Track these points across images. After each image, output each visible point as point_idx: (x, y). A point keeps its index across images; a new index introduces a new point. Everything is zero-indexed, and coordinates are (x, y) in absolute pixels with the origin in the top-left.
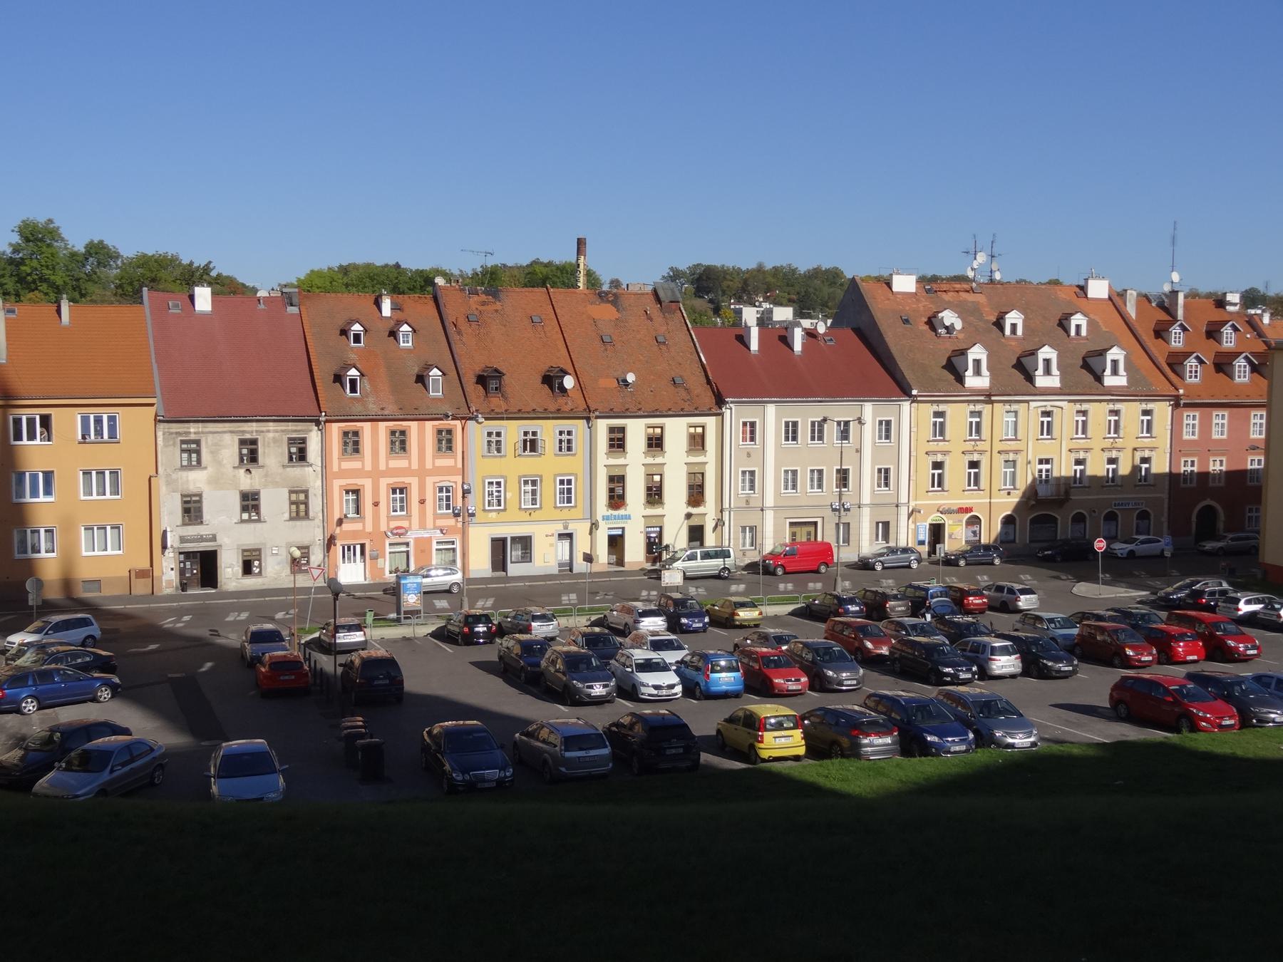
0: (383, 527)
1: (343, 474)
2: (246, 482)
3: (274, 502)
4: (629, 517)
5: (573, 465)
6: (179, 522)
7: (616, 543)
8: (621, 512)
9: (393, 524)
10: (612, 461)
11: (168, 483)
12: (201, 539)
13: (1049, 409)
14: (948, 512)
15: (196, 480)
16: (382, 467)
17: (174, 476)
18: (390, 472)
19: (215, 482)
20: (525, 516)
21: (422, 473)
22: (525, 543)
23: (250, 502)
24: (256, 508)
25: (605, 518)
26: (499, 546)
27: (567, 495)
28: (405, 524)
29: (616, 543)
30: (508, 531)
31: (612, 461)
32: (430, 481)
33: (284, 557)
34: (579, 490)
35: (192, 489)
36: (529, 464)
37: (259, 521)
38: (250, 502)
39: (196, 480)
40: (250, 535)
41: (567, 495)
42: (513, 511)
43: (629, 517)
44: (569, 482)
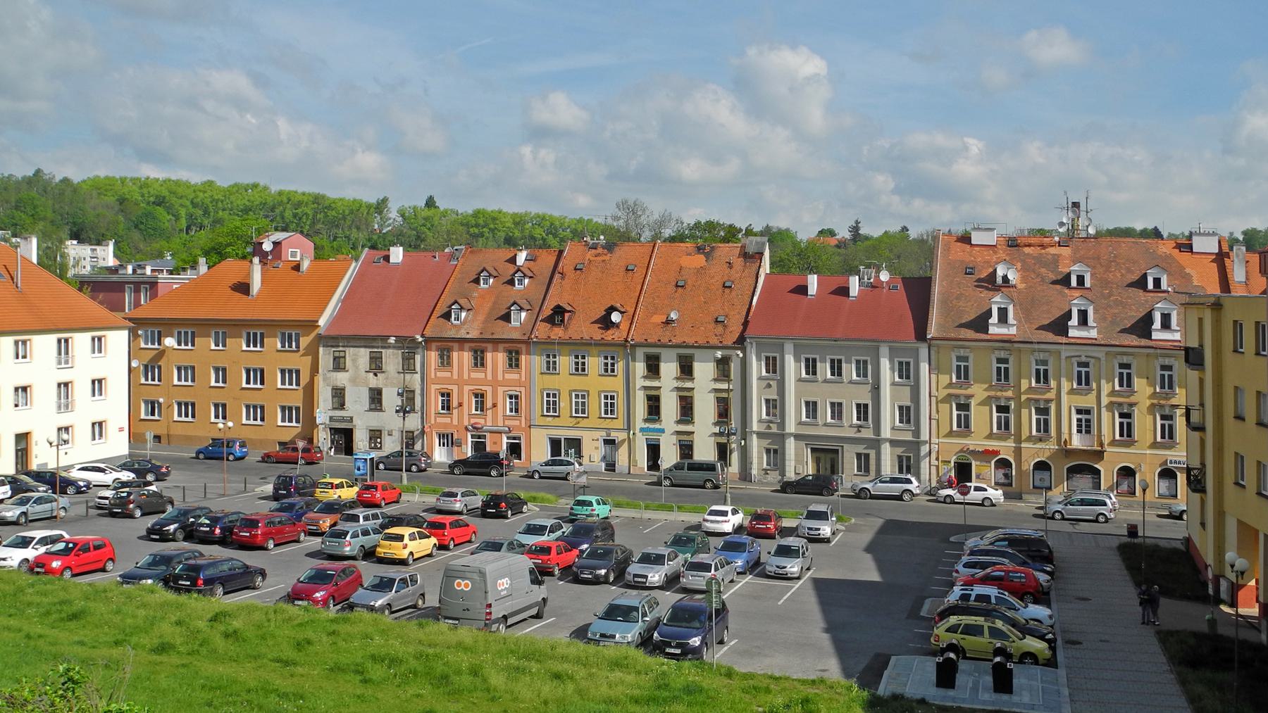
0: (466, 423)
1: (438, 381)
2: (374, 382)
3: (391, 399)
4: (663, 431)
5: (615, 384)
6: (330, 406)
7: (654, 451)
8: (657, 426)
9: (473, 421)
10: (648, 383)
11: (324, 380)
12: (343, 420)
13: (1084, 359)
14: (973, 453)
15: (341, 378)
16: (466, 377)
17: (329, 375)
18: (470, 381)
19: (354, 381)
20: (572, 422)
21: (495, 384)
22: (575, 444)
23: (376, 398)
24: (380, 402)
25: (642, 430)
26: (555, 444)
27: (610, 408)
28: (482, 421)
29: (654, 451)
30: (562, 434)
31: (648, 383)
32: (500, 390)
33: (396, 435)
34: (620, 403)
35: (339, 384)
36: (578, 382)
37: (381, 410)
38: (376, 398)
39: (341, 378)
40: (375, 420)
41: (610, 408)
42: (565, 419)
43: (663, 431)
44: (612, 398)
